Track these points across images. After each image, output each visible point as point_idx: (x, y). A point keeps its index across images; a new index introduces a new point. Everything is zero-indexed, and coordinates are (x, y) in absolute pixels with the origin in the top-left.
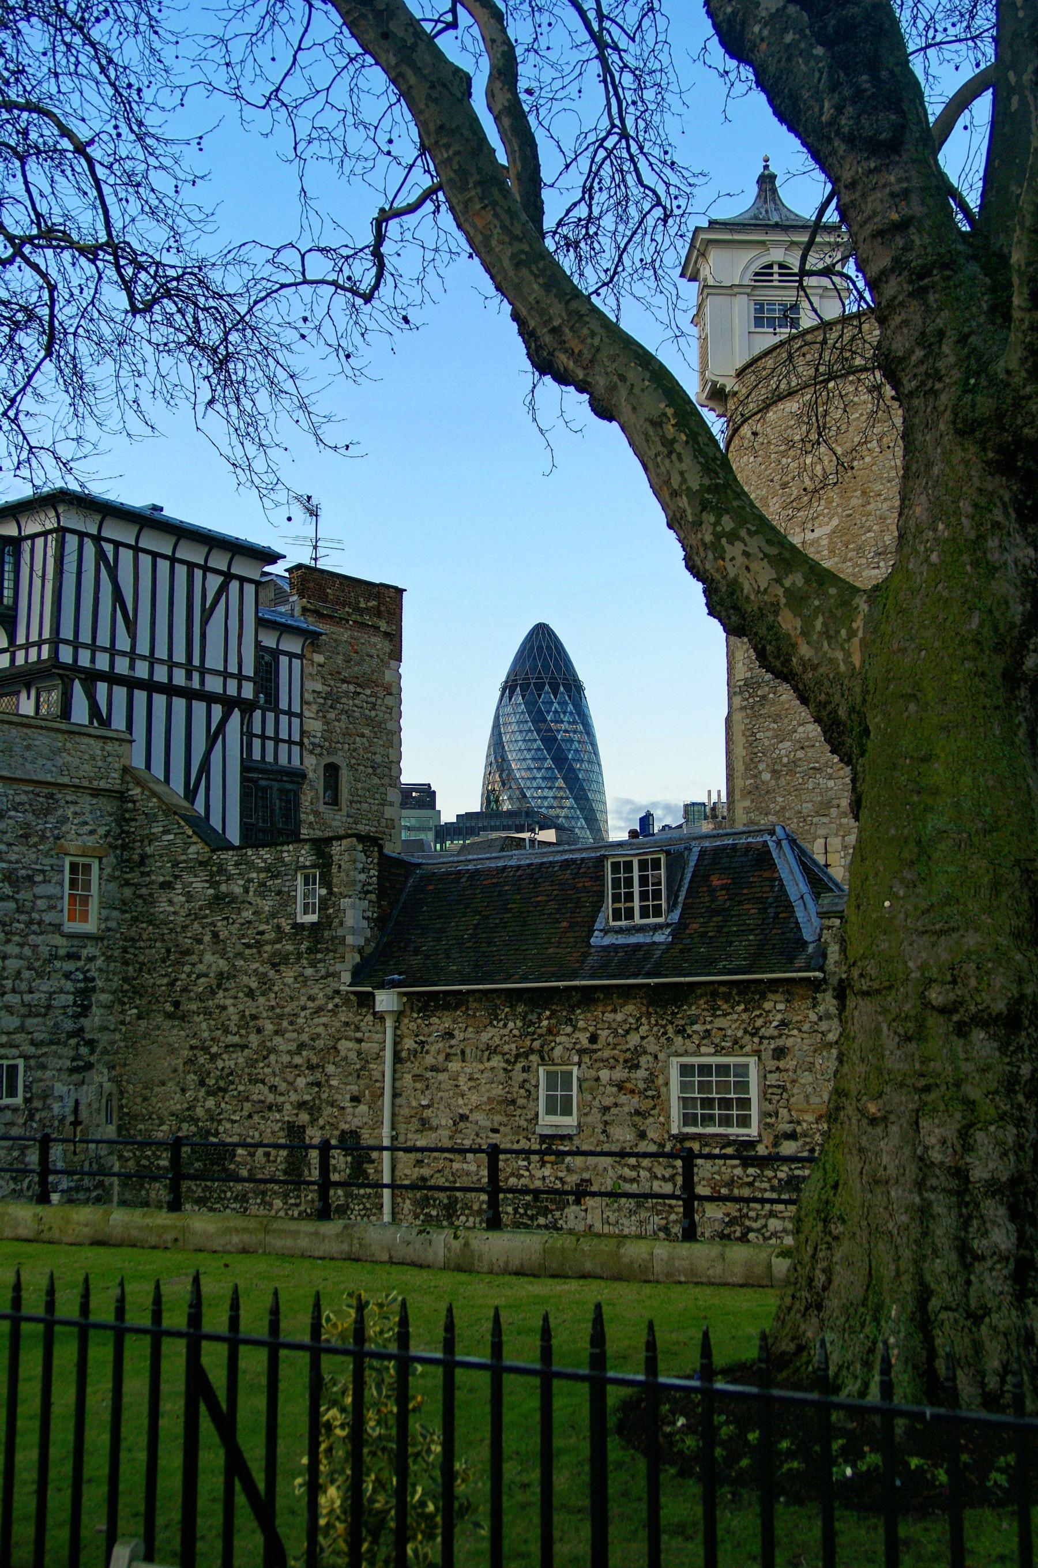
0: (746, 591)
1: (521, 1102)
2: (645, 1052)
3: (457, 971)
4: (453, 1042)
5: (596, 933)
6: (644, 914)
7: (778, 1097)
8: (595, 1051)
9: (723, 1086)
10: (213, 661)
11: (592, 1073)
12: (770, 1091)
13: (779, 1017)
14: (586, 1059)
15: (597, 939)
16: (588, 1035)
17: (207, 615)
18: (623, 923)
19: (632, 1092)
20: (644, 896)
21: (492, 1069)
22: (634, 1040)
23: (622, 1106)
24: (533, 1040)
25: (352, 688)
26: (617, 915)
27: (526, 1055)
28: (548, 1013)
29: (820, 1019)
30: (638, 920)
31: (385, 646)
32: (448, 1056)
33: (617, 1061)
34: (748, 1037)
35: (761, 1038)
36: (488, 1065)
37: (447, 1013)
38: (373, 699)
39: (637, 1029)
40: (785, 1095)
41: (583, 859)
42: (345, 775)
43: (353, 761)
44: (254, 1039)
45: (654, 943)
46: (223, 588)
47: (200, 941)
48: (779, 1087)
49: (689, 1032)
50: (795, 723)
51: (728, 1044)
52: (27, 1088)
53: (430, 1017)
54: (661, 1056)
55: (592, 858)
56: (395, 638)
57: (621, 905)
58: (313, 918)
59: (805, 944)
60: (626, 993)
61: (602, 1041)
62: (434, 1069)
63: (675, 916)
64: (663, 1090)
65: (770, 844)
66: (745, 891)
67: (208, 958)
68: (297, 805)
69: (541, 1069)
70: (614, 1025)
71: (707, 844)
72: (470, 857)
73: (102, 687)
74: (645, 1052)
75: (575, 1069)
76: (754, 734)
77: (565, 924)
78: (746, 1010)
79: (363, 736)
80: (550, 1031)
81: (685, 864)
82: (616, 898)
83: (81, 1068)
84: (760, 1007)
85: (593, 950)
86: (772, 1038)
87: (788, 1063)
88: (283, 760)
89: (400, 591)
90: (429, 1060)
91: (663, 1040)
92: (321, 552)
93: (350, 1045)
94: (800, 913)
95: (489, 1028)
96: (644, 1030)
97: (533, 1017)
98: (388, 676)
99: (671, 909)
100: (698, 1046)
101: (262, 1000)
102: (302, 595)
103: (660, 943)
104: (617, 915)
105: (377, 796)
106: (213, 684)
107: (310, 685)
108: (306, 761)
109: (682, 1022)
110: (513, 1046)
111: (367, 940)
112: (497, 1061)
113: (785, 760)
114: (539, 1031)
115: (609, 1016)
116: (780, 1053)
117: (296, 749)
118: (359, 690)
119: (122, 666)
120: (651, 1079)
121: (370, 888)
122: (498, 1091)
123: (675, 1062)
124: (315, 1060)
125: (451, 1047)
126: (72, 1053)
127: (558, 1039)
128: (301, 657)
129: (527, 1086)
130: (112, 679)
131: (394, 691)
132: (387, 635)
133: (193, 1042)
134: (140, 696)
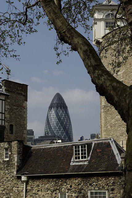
0: (104, 87)
3: (40, 171)
4: (39, 187)
6: (82, 158)
11: (71, 194)
13: (113, 181)
14: (69, 191)
15: (72, 164)
18: (77, 160)
20: (82, 154)
24: (57, 187)
26: (76, 158)
27: (56, 190)
29: (122, 182)
30: (81, 159)
31: (24, 98)
32: (38, 191)
33: (76, 191)
34: (105, 186)
35: (109, 186)
36: (47, 193)
38: (21, 110)
39: (81, 184)
41: (68, 146)
42: (14, 127)
43: (16, 124)
51: (101, 187)
54: (86, 190)
55: (70, 145)
56: (26, 96)
57: (77, 156)
58: (8, 159)
59: (118, 165)
61: (73, 187)
63: (89, 158)
65: (110, 142)
68: (3, 134)
69: (59, 193)
70: (76, 183)
71: (96, 142)
72: (43, 145)
74: (82, 189)
77: (64, 160)
78: (105, 180)
80: (61, 185)
81: (92, 146)
82: (76, 154)
84: (108, 179)
85: (71, 166)
86: (111, 186)
89: (27, 86)
90: (34, 192)
94: (117, 158)
95: (48, 184)
96: (82, 184)
97: (57, 181)
98: (24, 105)
99: (88, 156)
100: (95, 188)
102: (5, 87)
104: (76, 158)
107: (7, 107)
108: (6, 124)
109: (91, 182)
111: (20, 164)
113: (113, 124)
115: (74, 181)
116: (113, 190)
117: (3, 121)
124: (8, 192)
128: (4, 100)
132: (24, 95)
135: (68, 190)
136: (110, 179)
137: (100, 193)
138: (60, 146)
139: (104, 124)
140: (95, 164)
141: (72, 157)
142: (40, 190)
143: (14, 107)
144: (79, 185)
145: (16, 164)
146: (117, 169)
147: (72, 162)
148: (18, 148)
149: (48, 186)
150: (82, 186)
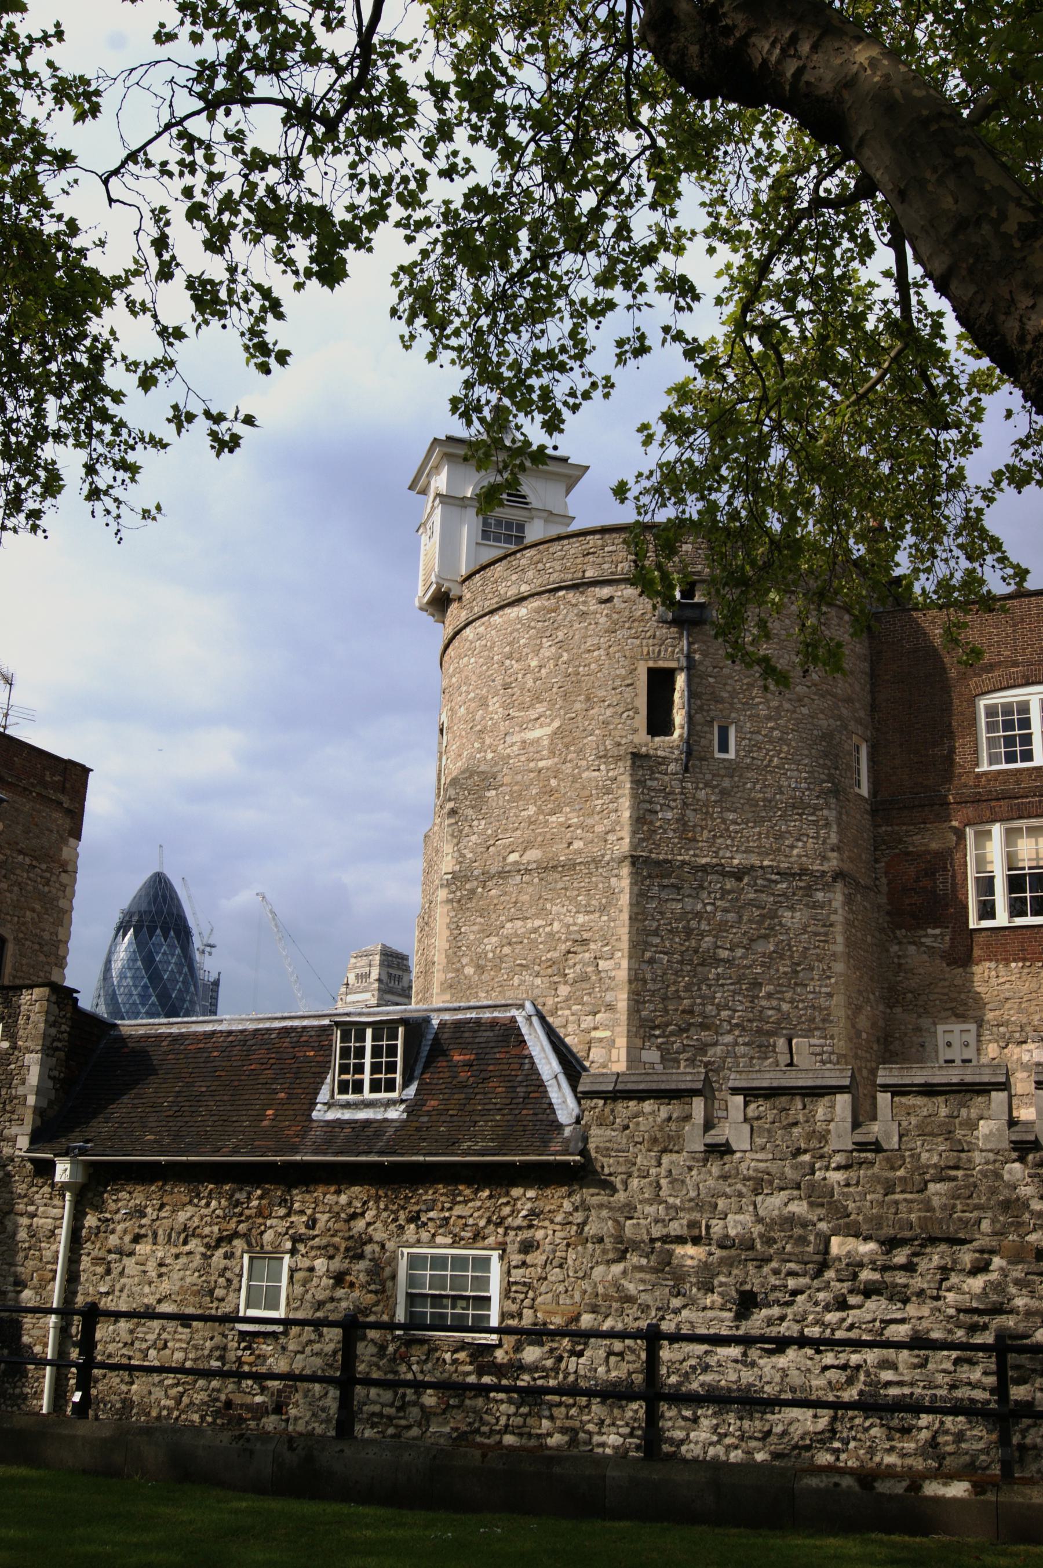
1: (219, 1293)
2: (370, 1240)
3: (155, 1141)
4: (144, 1221)
5: (319, 1106)
6: (375, 1087)
7: (522, 1296)
8: (314, 1237)
11: (305, 1263)
12: (514, 1288)
13: (529, 1205)
14: (301, 1247)
15: (318, 1114)
16: (305, 1219)
18: (350, 1097)
19: (352, 1285)
20: (376, 1068)
21: (189, 1253)
23: (340, 1300)
24: (240, 1222)
25: (28, 861)
27: (229, 1239)
28: (259, 1192)
29: (576, 1209)
31: (67, 823)
32: (137, 1239)
33: (337, 1249)
34: (492, 1227)
35: (507, 1228)
36: (187, 1248)
37: (140, 1188)
38: (48, 875)
39: (363, 1214)
40: (531, 1294)
41: (304, 1028)
43: (21, 935)
45: (386, 1120)
48: (524, 1284)
49: (424, 1219)
50: (503, 918)
53: (118, 1191)
54: (390, 1245)
55: (313, 1027)
59: (560, 1127)
61: (320, 1225)
62: (120, 1252)
64: (389, 1284)
65: (519, 1019)
66: (491, 1068)
69: (246, 1257)
75: (287, 1257)
76: (458, 927)
77: (282, 1095)
79: (33, 910)
80: (260, 1213)
82: (344, 1069)
84: (507, 1194)
85: (315, 1125)
89: (85, 771)
90: (113, 1240)
91: (392, 1227)
92: (11, 720)
94: (554, 1095)
95: (189, 1208)
96: (369, 1215)
97: (241, 1196)
98: (66, 853)
100: (434, 1235)
103: (393, 1121)
104: (343, 1088)
105: (42, 974)
110: (216, 1229)
111: (51, 1103)
113: (490, 955)
114: (247, 1212)
115: (330, 1198)
118: (34, 863)
121: (59, 1045)
125: (141, 1226)
127: (269, 1223)
129: (228, 1274)
131: (70, 868)
135: (296, 1239)
136: (516, 1192)
137: (460, 1262)
138: (261, 1026)
139: (447, 956)
140: (443, 1118)
141: (322, 1083)
142: (145, 1236)
143: (20, 858)
144: (354, 1216)
145: (31, 1100)
146: (555, 1147)
147: (325, 1104)
148: (46, 1021)
149: (189, 1214)
150: (369, 1224)
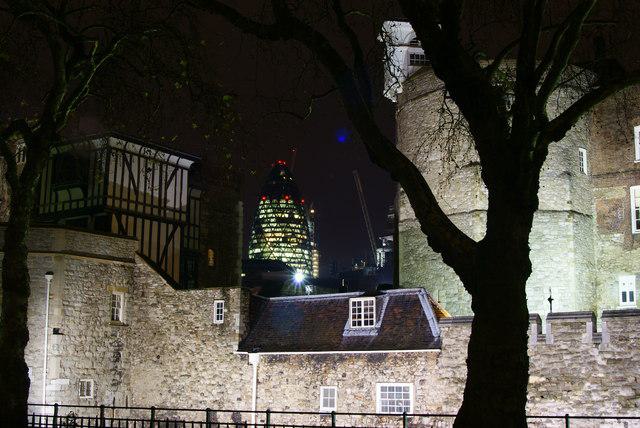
9: (399, 396)
10: (170, 204)
14: (341, 383)
17: (167, 185)
22: (361, 377)
26: (354, 324)
44: (193, 373)
46: (174, 173)
47: (169, 330)
52: (95, 392)
57: (356, 320)
58: (221, 322)
60: (358, 357)
63: (379, 325)
67: (173, 337)
73: (124, 217)
82: (354, 317)
83: (116, 384)
87: (425, 386)
88: (191, 246)
90: (272, 384)
93: (237, 376)
99: (377, 322)
101: (198, 356)
104: (354, 324)
106: (169, 214)
112: (302, 383)
119: (132, 207)
120: (368, 392)
122: (303, 397)
123: (379, 386)
124: (221, 383)
126: (112, 378)
130: (128, 213)
133: (166, 374)
134: (139, 221)
145: (237, 331)
